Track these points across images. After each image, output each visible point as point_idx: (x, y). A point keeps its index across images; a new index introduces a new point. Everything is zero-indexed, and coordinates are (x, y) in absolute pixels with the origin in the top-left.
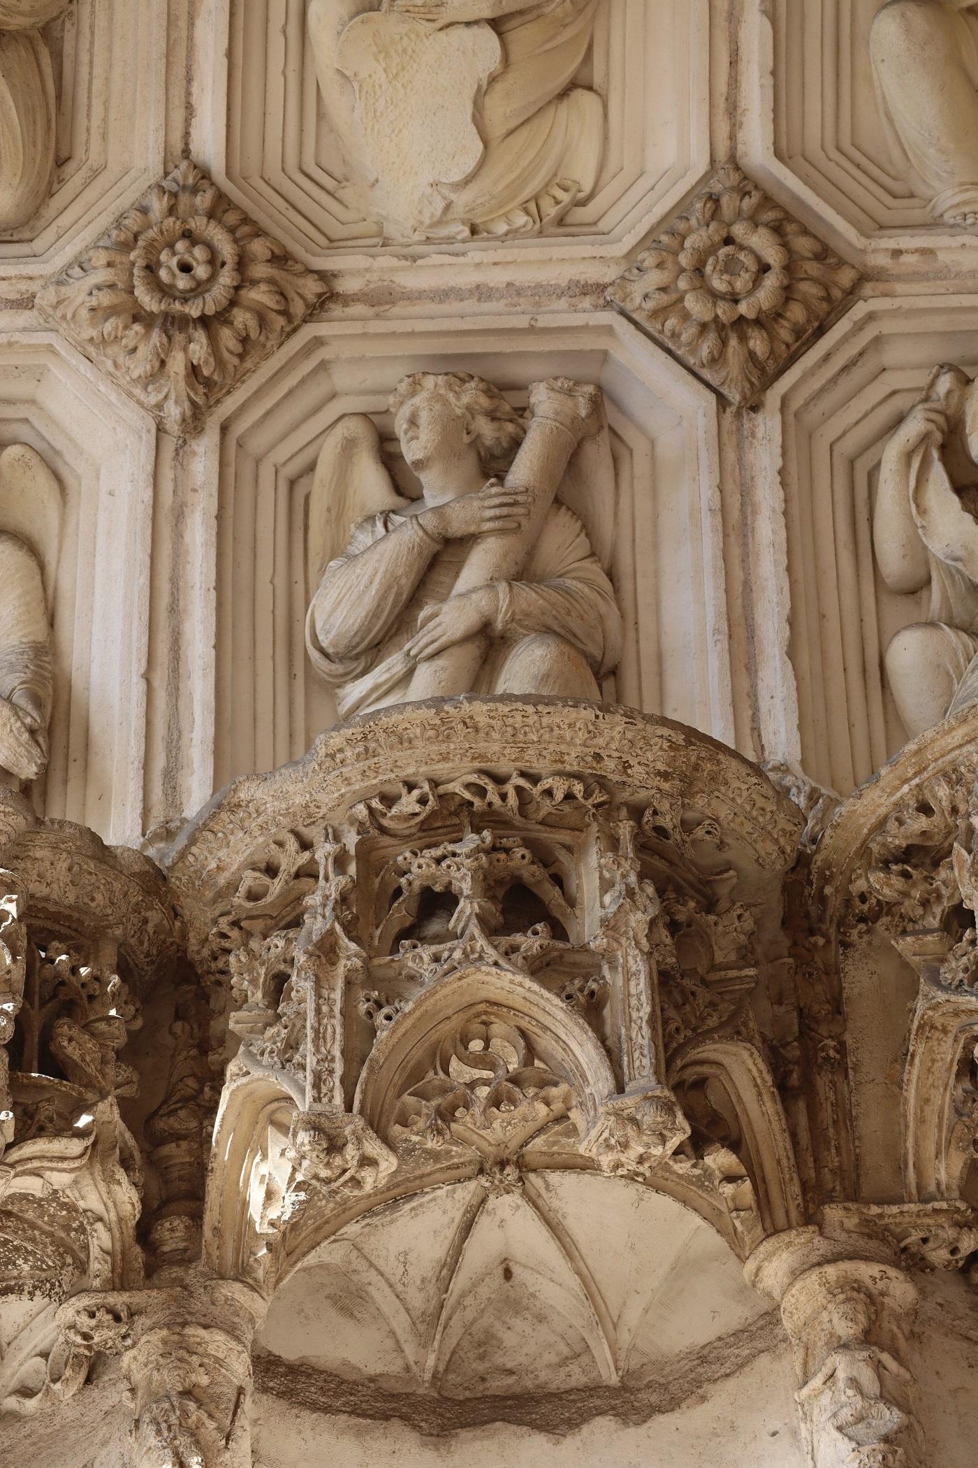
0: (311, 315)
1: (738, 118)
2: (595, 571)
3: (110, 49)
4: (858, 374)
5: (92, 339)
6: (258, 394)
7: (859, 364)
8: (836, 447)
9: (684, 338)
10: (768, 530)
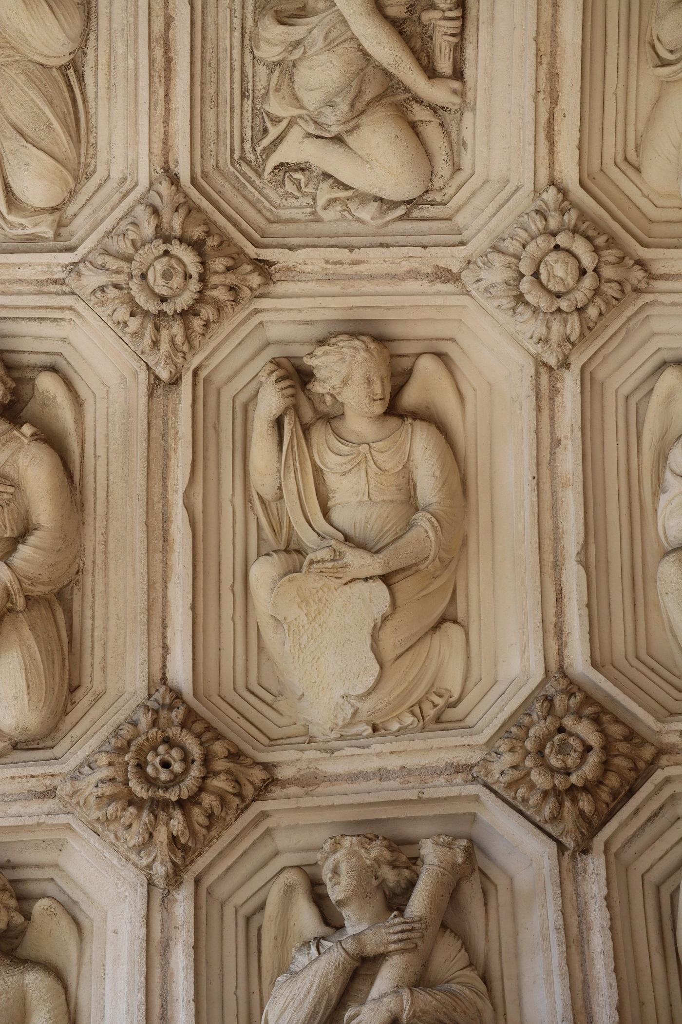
0: (258, 795)
1: (564, 639)
2: (472, 976)
3: (106, 606)
4: (661, 822)
5: (99, 819)
6: (221, 855)
7: (660, 815)
8: (645, 877)
9: (531, 802)
10: (599, 941)
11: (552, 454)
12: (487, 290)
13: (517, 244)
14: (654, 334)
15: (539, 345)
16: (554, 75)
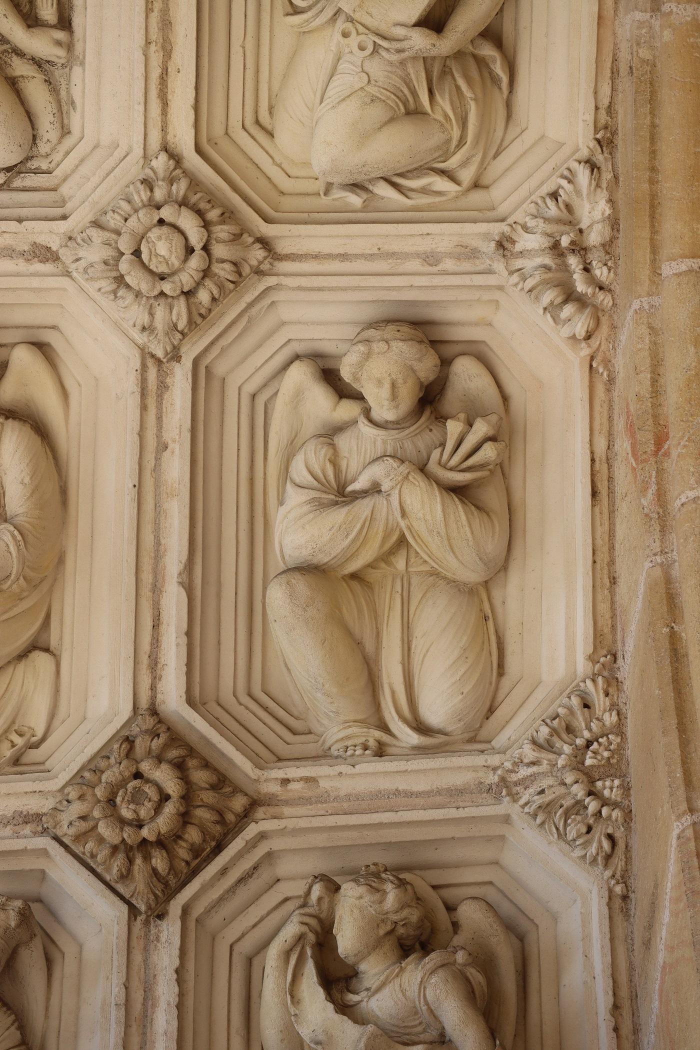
1: (158, 672)
4: (254, 885)
7: (255, 876)
8: (237, 948)
9: (99, 858)
11: (158, 459)
12: (85, 270)
13: (119, 218)
14: (284, 324)
15: (145, 334)
16: (166, 24)
